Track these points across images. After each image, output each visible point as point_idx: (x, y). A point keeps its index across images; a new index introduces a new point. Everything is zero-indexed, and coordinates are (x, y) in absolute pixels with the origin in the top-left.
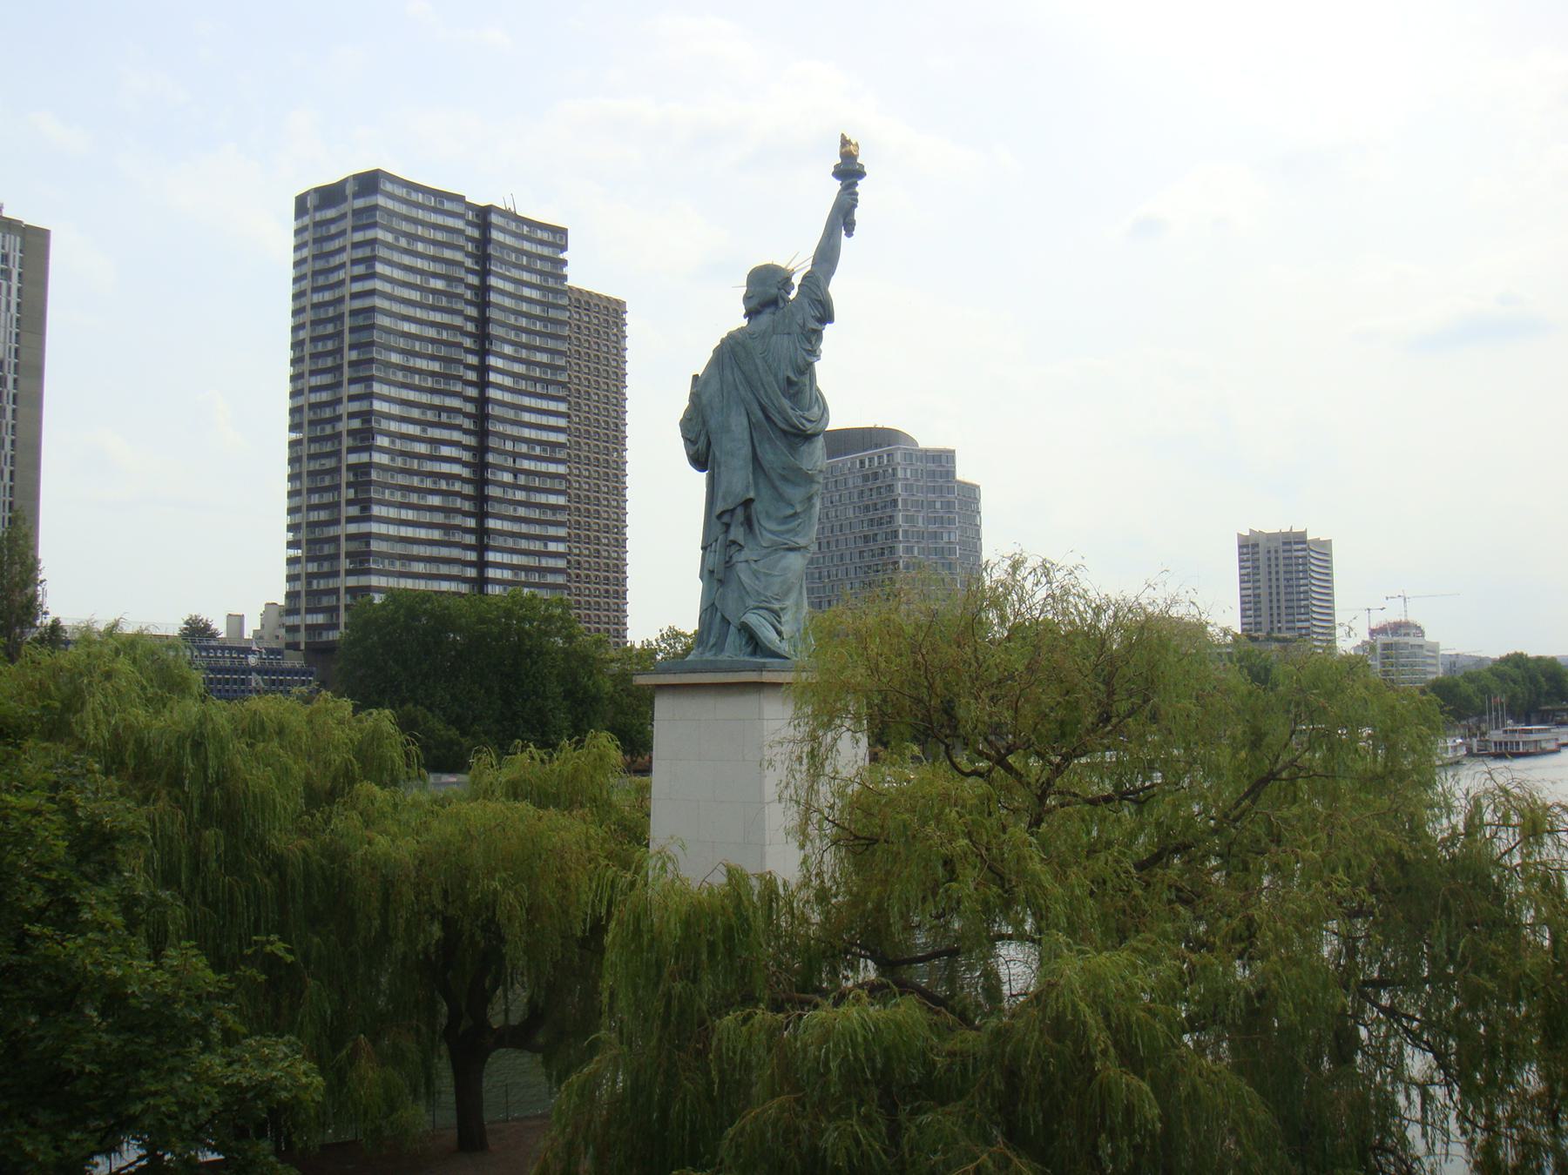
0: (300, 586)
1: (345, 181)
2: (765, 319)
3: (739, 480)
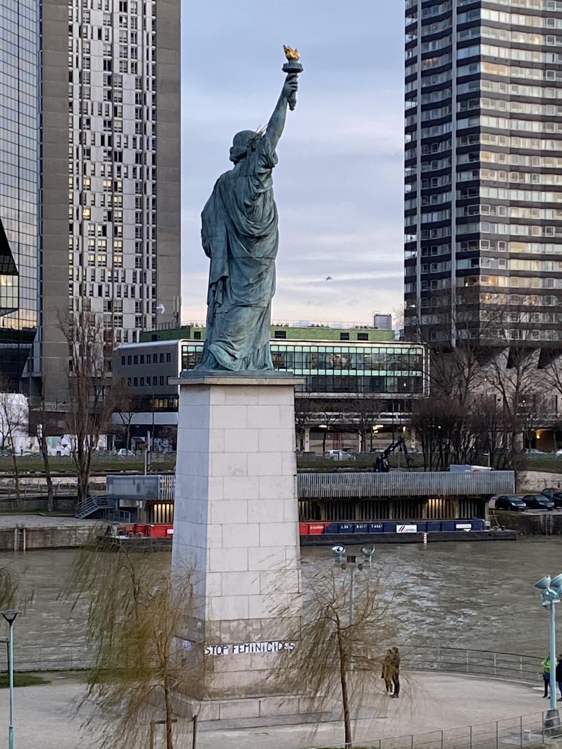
2: (239, 165)
3: (221, 261)
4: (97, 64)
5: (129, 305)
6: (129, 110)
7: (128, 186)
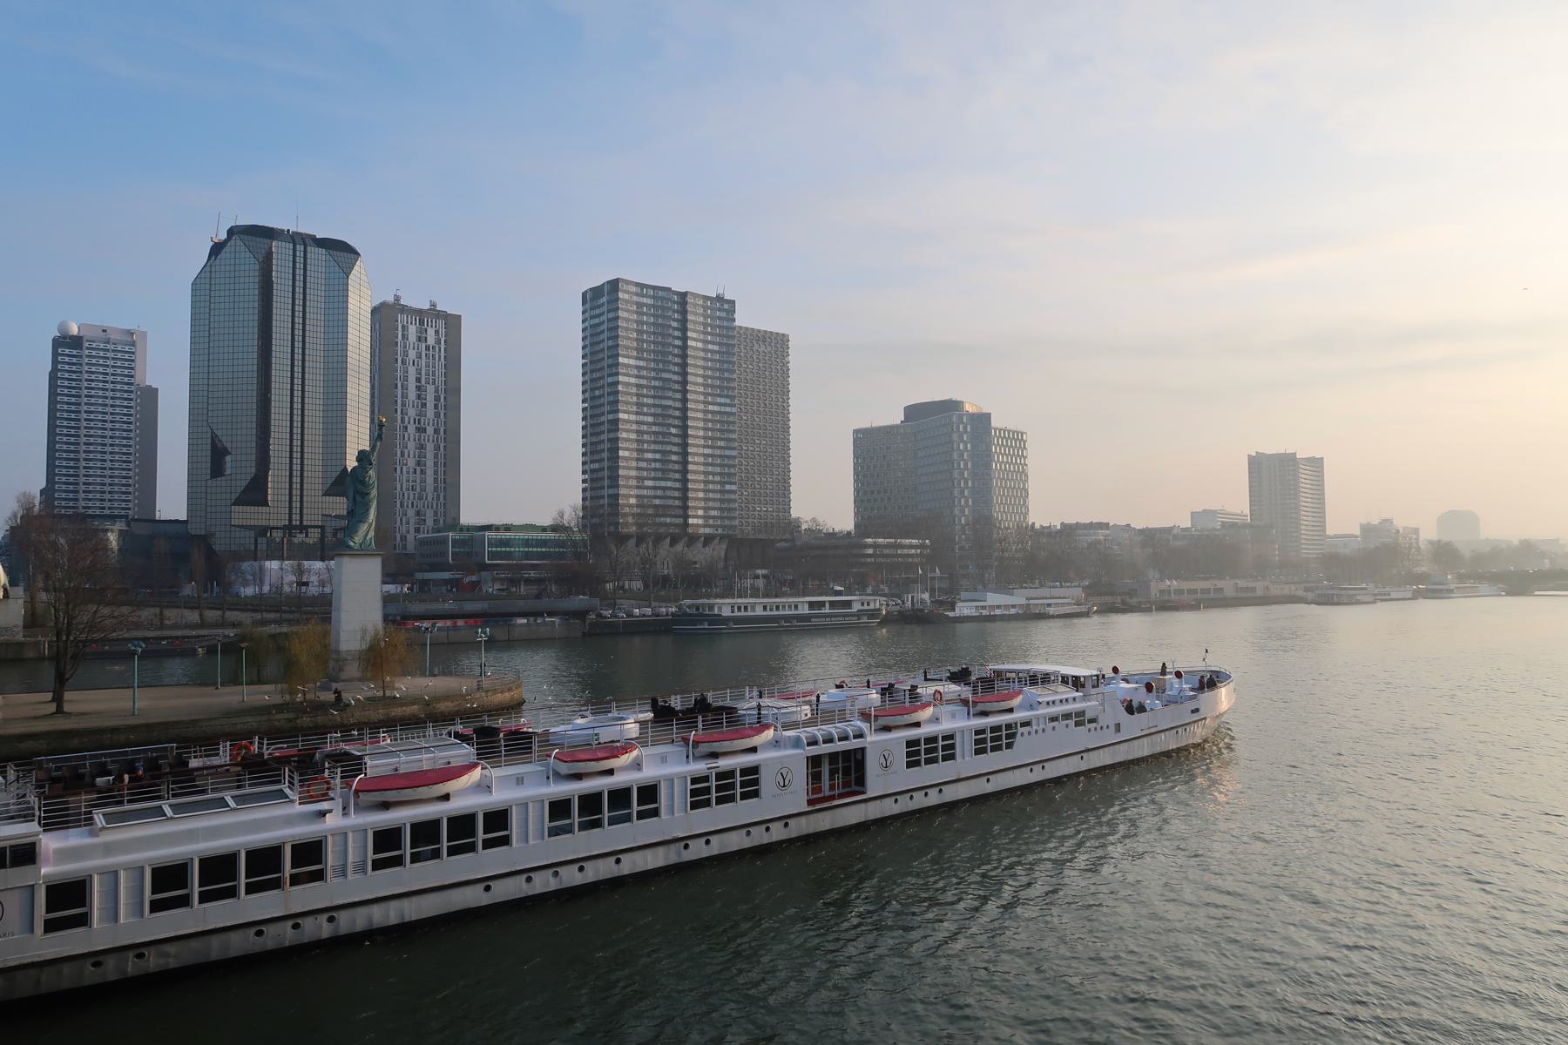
5: (429, 515)
7: (430, 446)
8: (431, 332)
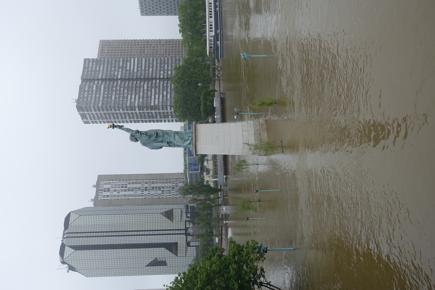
0: (174, 119)
1: (79, 114)
4: (125, 193)
6: (136, 186)
8: (105, 186)
